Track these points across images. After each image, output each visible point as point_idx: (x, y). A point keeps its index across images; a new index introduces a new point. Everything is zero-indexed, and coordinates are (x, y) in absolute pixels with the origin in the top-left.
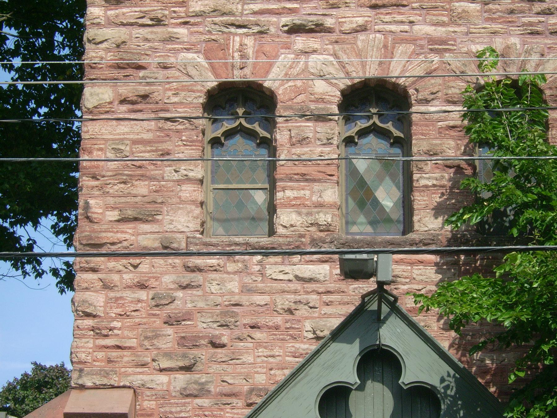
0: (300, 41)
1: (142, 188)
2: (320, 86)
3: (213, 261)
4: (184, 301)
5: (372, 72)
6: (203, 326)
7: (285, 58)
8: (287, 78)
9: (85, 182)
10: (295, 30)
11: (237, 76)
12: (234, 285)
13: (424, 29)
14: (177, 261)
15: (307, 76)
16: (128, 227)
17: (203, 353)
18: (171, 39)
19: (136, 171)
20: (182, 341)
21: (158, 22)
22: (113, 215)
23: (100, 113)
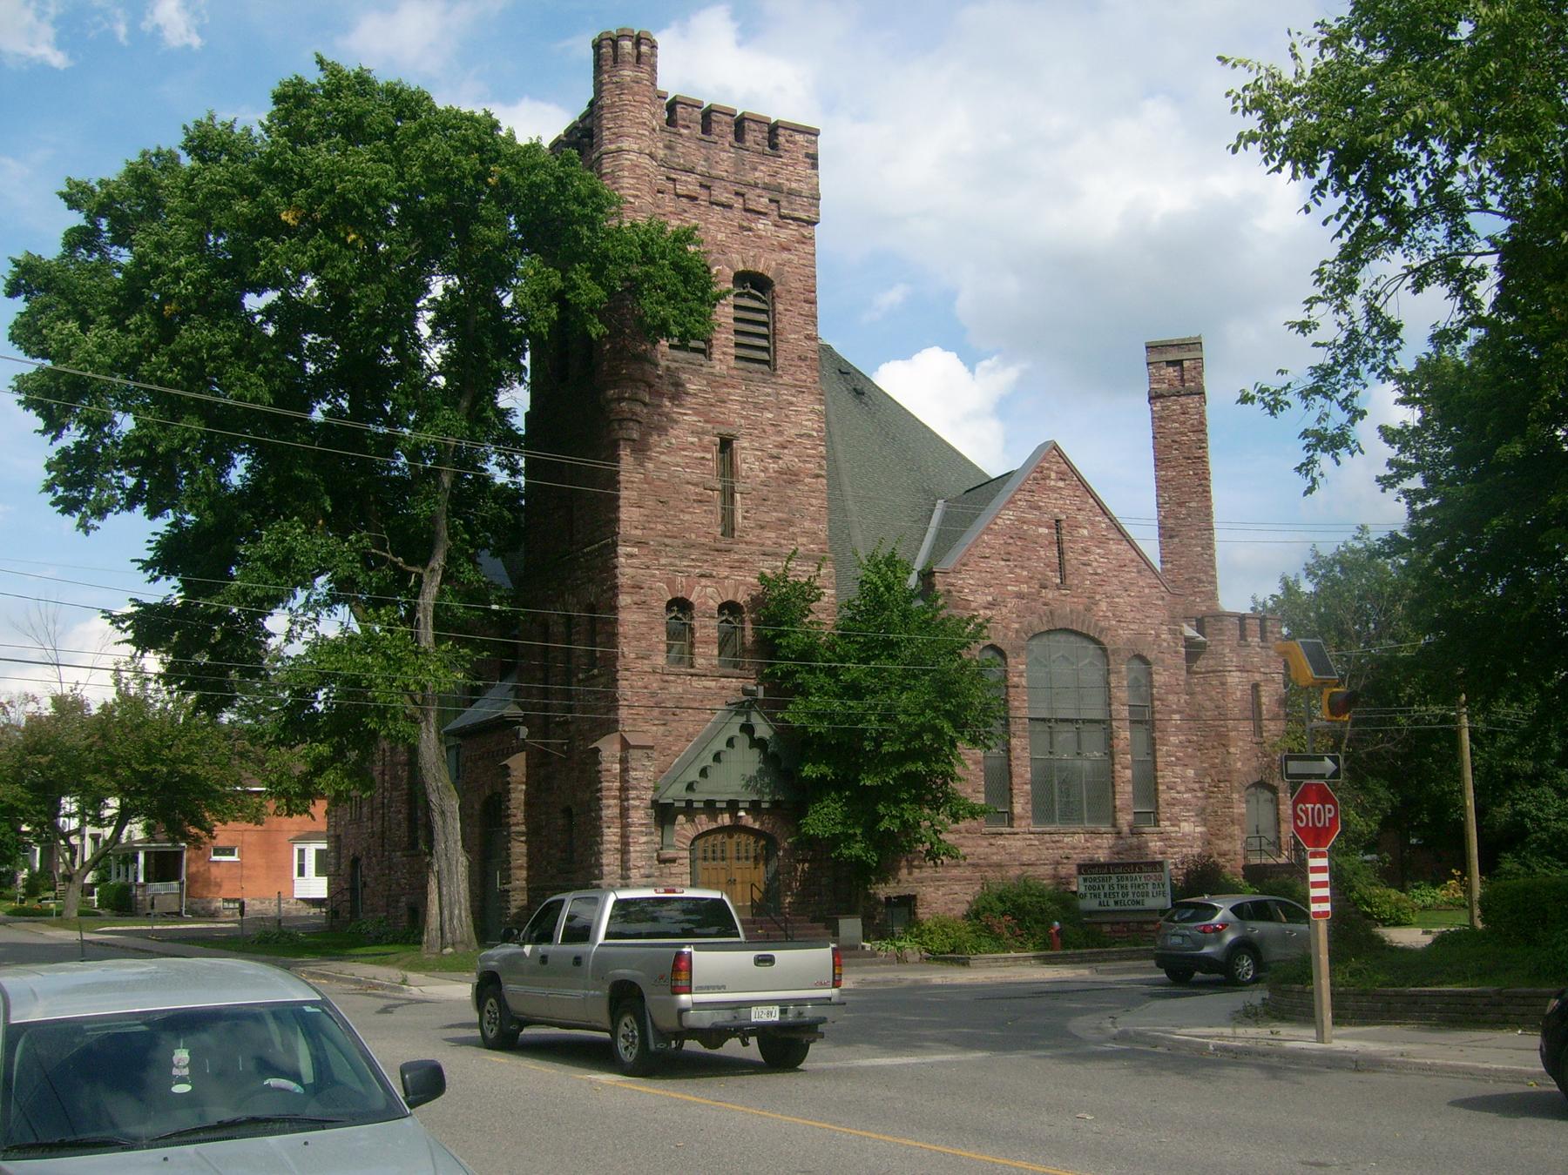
0: (704, 581)
1: (644, 644)
2: (711, 602)
4: (662, 695)
5: (730, 598)
7: (698, 588)
9: (622, 640)
10: (702, 576)
14: (658, 677)
15: (707, 597)
18: (653, 576)
19: (640, 637)
22: (633, 656)
23: (626, 607)
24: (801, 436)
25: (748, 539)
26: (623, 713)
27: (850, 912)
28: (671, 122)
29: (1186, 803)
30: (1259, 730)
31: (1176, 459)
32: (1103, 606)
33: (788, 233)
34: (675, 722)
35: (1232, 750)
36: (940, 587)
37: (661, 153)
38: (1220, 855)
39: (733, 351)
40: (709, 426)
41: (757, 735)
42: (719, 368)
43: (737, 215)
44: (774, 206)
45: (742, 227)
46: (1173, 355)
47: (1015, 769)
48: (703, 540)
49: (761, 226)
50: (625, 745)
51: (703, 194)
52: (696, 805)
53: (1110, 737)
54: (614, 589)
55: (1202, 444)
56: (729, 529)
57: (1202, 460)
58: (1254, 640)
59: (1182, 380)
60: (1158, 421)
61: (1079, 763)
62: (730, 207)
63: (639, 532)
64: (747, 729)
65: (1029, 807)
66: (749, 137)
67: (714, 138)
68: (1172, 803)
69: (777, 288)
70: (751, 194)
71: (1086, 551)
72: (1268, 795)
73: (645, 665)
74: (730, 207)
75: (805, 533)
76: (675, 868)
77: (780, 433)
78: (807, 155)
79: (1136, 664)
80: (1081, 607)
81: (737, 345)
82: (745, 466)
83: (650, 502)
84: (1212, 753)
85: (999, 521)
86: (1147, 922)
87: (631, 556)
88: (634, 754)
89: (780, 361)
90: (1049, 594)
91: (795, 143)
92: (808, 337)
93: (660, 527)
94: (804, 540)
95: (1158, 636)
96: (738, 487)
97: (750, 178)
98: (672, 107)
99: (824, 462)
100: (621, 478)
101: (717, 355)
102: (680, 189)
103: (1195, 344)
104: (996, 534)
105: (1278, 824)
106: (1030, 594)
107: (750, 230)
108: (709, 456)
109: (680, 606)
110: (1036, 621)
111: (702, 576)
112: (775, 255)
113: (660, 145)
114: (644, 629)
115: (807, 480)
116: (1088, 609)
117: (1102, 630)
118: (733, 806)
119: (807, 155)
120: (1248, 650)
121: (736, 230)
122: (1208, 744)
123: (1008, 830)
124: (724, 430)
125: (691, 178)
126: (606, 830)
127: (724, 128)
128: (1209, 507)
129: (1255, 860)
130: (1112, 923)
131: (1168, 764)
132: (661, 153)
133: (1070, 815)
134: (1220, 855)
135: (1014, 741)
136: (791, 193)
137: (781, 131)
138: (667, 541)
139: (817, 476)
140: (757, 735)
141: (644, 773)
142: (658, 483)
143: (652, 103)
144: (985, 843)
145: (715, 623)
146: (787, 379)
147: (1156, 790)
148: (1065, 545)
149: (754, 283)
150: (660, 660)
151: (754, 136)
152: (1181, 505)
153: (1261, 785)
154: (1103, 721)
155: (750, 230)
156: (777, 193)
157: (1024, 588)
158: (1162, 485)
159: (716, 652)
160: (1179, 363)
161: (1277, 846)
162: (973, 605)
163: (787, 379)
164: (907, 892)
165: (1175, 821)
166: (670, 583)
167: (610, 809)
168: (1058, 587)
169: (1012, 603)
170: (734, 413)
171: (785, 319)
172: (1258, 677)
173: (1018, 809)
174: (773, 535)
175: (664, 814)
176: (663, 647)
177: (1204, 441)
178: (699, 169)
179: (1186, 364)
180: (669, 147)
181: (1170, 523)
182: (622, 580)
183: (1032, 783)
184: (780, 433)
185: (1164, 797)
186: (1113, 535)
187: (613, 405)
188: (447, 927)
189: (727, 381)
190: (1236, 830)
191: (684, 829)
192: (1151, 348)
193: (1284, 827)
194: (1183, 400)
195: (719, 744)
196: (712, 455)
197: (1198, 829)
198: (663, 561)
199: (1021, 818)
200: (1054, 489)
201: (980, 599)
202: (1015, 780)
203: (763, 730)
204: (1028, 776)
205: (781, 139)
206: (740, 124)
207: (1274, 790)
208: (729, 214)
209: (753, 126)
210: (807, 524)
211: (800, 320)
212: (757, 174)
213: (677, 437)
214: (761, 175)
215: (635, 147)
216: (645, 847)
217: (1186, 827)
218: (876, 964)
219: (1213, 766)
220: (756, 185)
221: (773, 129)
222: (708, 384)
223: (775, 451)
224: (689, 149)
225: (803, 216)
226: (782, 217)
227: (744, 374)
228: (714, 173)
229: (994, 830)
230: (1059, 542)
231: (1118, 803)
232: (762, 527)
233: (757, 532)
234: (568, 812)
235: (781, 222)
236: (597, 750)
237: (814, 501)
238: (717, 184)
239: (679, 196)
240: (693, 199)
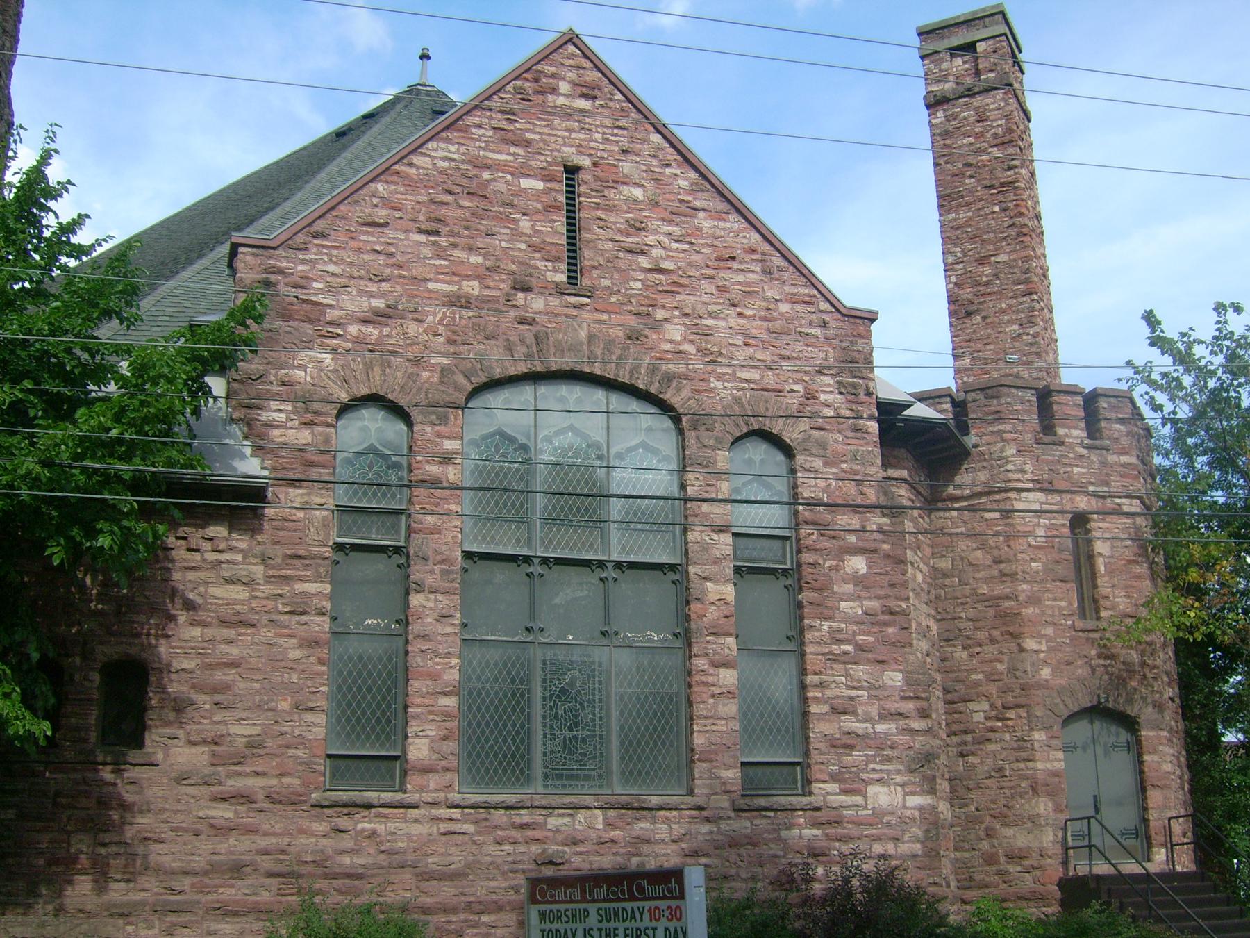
29: (881, 745)
30: (1090, 603)
31: (971, 191)
32: (675, 332)
35: (1030, 644)
38: (1010, 857)
46: (958, 39)
53: (685, 597)
58: (1074, 434)
59: (978, 73)
60: (942, 141)
61: (599, 655)
65: (451, 746)
68: (847, 743)
72: (1124, 736)
79: (758, 452)
80: (618, 332)
84: (990, 651)
95: (810, 396)
104: (411, 184)
105: (1142, 788)
106: (484, 300)
116: (635, 336)
117: (669, 378)
120: (1058, 451)
122: (982, 636)
129: (1081, 867)
131: (834, 659)
133: (574, 762)
134: (1010, 857)
135: (416, 600)
144: (320, 827)
147: (805, 714)
148: (583, 215)
152: (981, 261)
153: (1097, 711)
154: (673, 568)
157: (472, 288)
158: (951, 236)
161: (1142, 834)
162: (331, 314)
165: (852, 783)
169: (435, 314)
172: (1082, 503)
173: (418, 750)
179: (981, 47)
181: (966, 293)
185: (821, 728)
186: (705, 200)
190: (1043, 806)
192: (925, 33)
193: (1154, 797)
194: (978, 101)
197: (915, 801)
199: (427, 770)
204: (453, 676)
207: (1130, 724)
217: (881, 796)
219: (992, 677)
229: (345, 796)
231: (699, 740)
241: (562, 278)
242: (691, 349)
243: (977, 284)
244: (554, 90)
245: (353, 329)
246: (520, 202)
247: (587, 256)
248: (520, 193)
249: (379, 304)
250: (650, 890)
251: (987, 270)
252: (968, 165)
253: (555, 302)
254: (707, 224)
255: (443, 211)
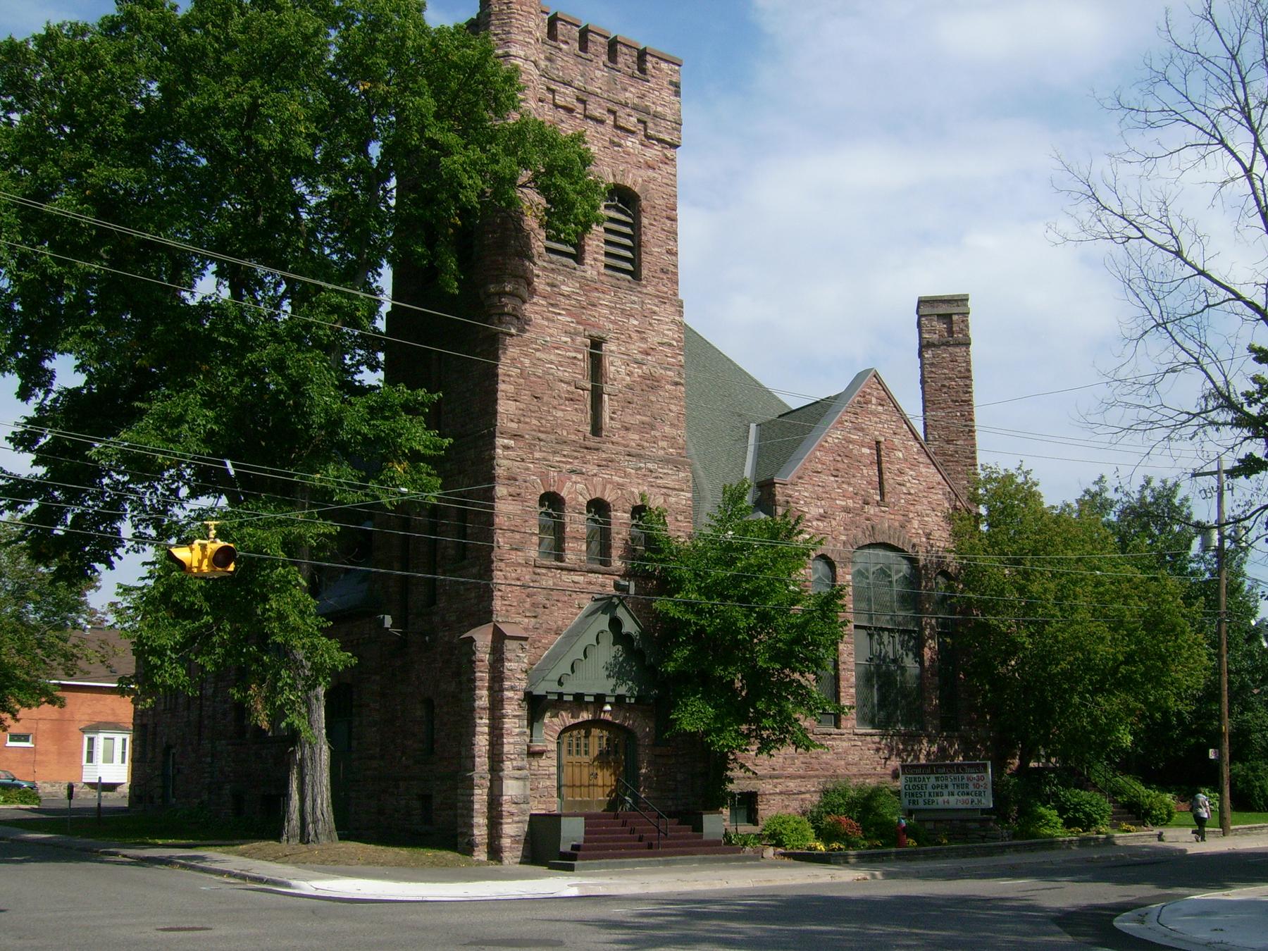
0: (574, 477)
1: (517, 536)
3: (544, 571)
5: (598, 495)
6: (540, 598)
7: (568, 484)
8: (569, 493)
10: (573, 471)
11: (552, 489)
12: (551, 583)
13: (616, 479)
15: (575, 493)
16: (513, 552)
17: (540, 610)
18: (528, 469)
20: (533, 605)
21: (523, 460)
23: (501, 498)
24: (662, 344)
25: (614, 439)
26: (497, 604)
27: (714, 807)
28: (552, 33)
31: (945, 401)
32: (916, 524)
33: (654, 153)
34: (545, 619)
36: (780, 498)
37: (543, 64)
39: (603, 258)
40: (581, 328)
41: (624, 630)
42: (590, 273)
43: (607, 130)
44: (641, 126)
45: (612, 142)
46: (943, 309)
47: (842, 673)
48: (573, 437)
49: (629, 144)
50: (499, 638)
51: (579, 108)
52: (566, 698)
54: (492, 479)
55: (967, 389)
56: (597, 429)
57: (968, 402)
59: (950, 332)
62: (602, 122)
63: (514, 425)
64: (615, 624)
66: (620, 59)
67: (589, 56)
69: (644, 203)
70: (621, 113)
71: (901, 473)
73: (518, 557)
74: (602, 122)
75: (665, 437)
76: (543, 762)
77: (644, 339)
78: (671, 83)
80: (897, 524)
81: (607, 254)
82: (612, 369)
83: (526, 396)
85: (830, 440)
86: (968, 820)
87: (506, 448)
88: (509, 645)
89: (644, 272)
90: (871, 510)
91: (660, 70)
92: (669, 252)
93: (534, 422)
94: (664, 444)
96: (607, 388)
97: (621, 97)
98: (553, 22)
99: (682, 371)
100: (500, 371)
101: (589, 260)
102: (560, 100)
103: (962, 300)
104: (827, 451)
106: (854, 508)
107: (620, 146)
108: (580, 356)
109: (552, 501)
110: (860, 535)
111: (573, 471)
112: (642, 172)
113: (542, 56)
114: (518, 521)
115: (668, 387)
118: (600, 699)
119: (671, 83)
121: (607, 144)
123: (837, 731)
124: (594, 333)
125: (569, 91)
126: (478, 721)
127: (598, 46)
128: (974, 445)
130: (936, 821)
132: (543, 64)
135: (841, 646)
136: (656, 116)
137: (649, 58)
138: (542, 436)
139: (677, 384)
140: (624, 630)
141: (516, 663)
142: (533, 379)
143: (537, 16)
145: (583, 518)
146: (650, 289)
148: (884, 465)
149: (625, 198)
150: (533, 553)
151: (626, 59)
152: (949, 442)
155: (620, 146)
156: (646, 115)
159: (584, 547)
160: (947, 318)
162: (808, 516)
163: (650, 289)
164: (750, 789)
166: (544, 477)
167: (482, 698)
168: (878, 504)
169: (841, 516)
170: (603, 318)
171: (649, 233)
174: (636, 437)
175: (536, 706)
176: (535, 539)
177: (969, 386)
178: (576, 83)
179: (955, 318)
180: (549, 59)
182: (499, 471)
183: (857, 686)
184: (644, 339)
187: (496, 300)
188: (309, 819)
189: (597, 286)
191: (553, 723)
192: (922, 302)
195: (589, 638)
196: (582, 357)
198: (537, 455)
200: (875, 414)
201: (813, 511)
202: (842, 684)
203: (629, 627)
204: (853, 679)
205: (649, 65)
206: (613, 46)
208: (601, 129)
209: (624, 50)
210: (667, 429)
211: (663, 236)
212: (627, 94)
213: (551, 336)
214: (630, 96)
215: (522, 53)
216: (517, 739)
218: (737, 860)
220: (626, 105)
221: (642, 55)
222: (581, 288)
223: (639, 357)
224: (567, 62)
225: (667, 138)
226: (648, 137)
227: (614, 281)
228: (589, 88)
230: (879, 463)
232: (627, 429)
233: (623, 433)
234: (429, 704)
235: (646, 143)
236: (471, 640)
237: (672, 407)
238: (592, 99)
239: (557, 106)
240: (569, 110)
241: (878, 498)
242: (920, 531)
243: (944, 454)
244: (870, 402)
245: (815, 523)
246: (863, 460)
247: (887, 488)
248: (863, 455)
249: (821, 511)
250: (968, 770)
251: (952, 448)
252: (944, 386)
253: (877, 509)
254: (924, 470)
255: (840, 465)
